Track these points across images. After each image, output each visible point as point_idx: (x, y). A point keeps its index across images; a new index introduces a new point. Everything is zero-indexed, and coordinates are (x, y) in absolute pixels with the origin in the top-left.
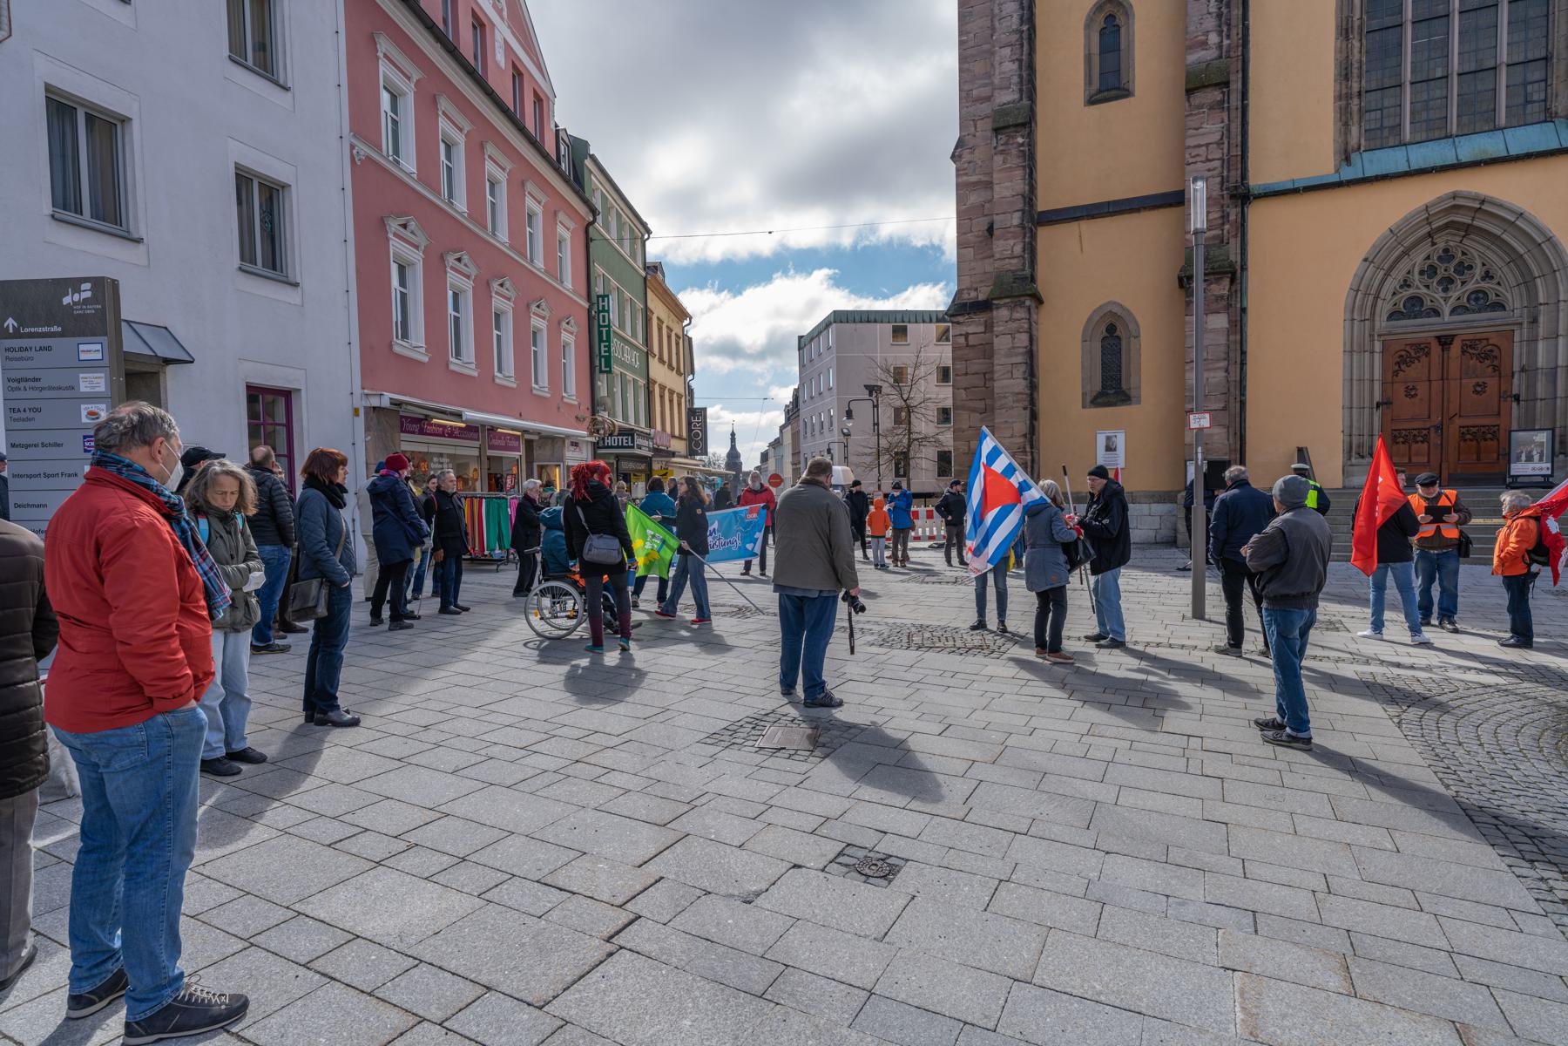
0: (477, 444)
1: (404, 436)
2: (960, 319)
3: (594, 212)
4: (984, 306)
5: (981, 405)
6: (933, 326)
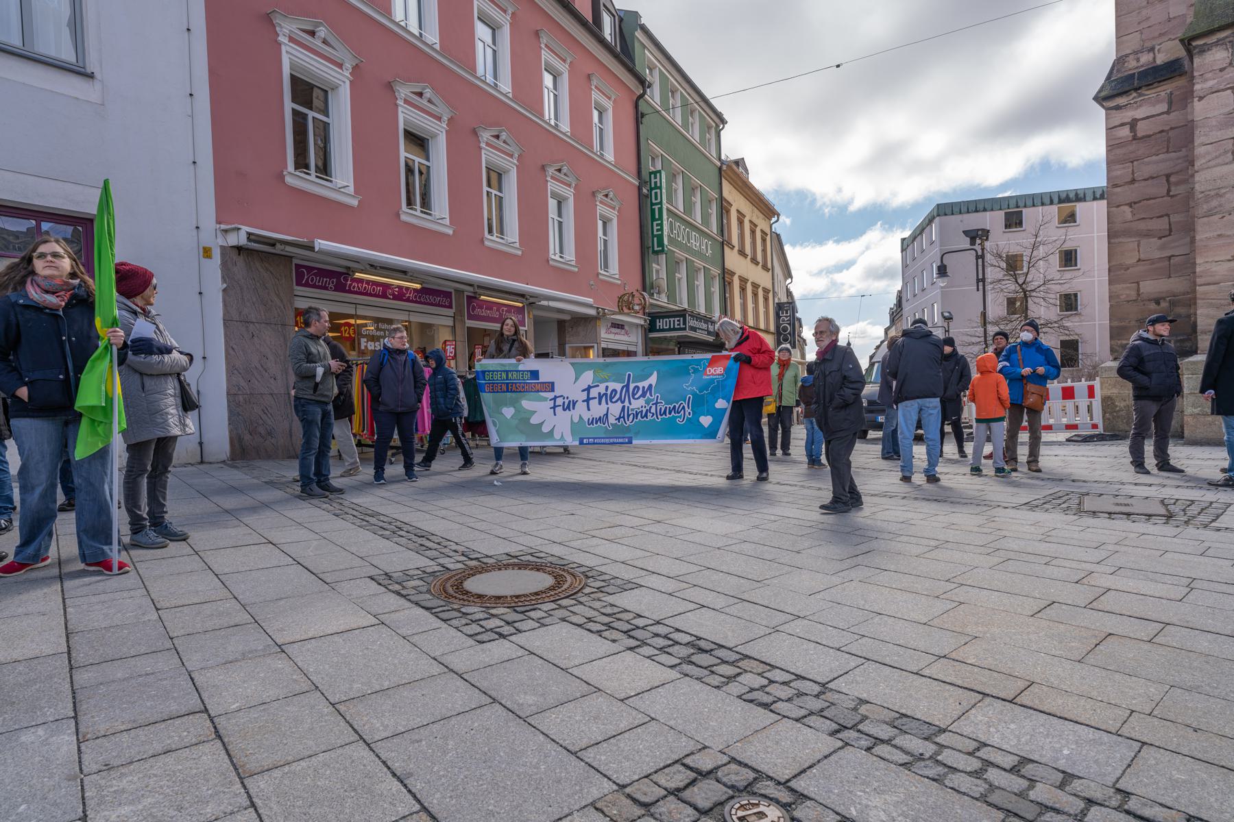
0: (451, 312)
1: (299, 290)
2: (1121, 101)
3: (642, 81)
4: (1172, 70)
5: (1163, 224)
6: (1055, 208)
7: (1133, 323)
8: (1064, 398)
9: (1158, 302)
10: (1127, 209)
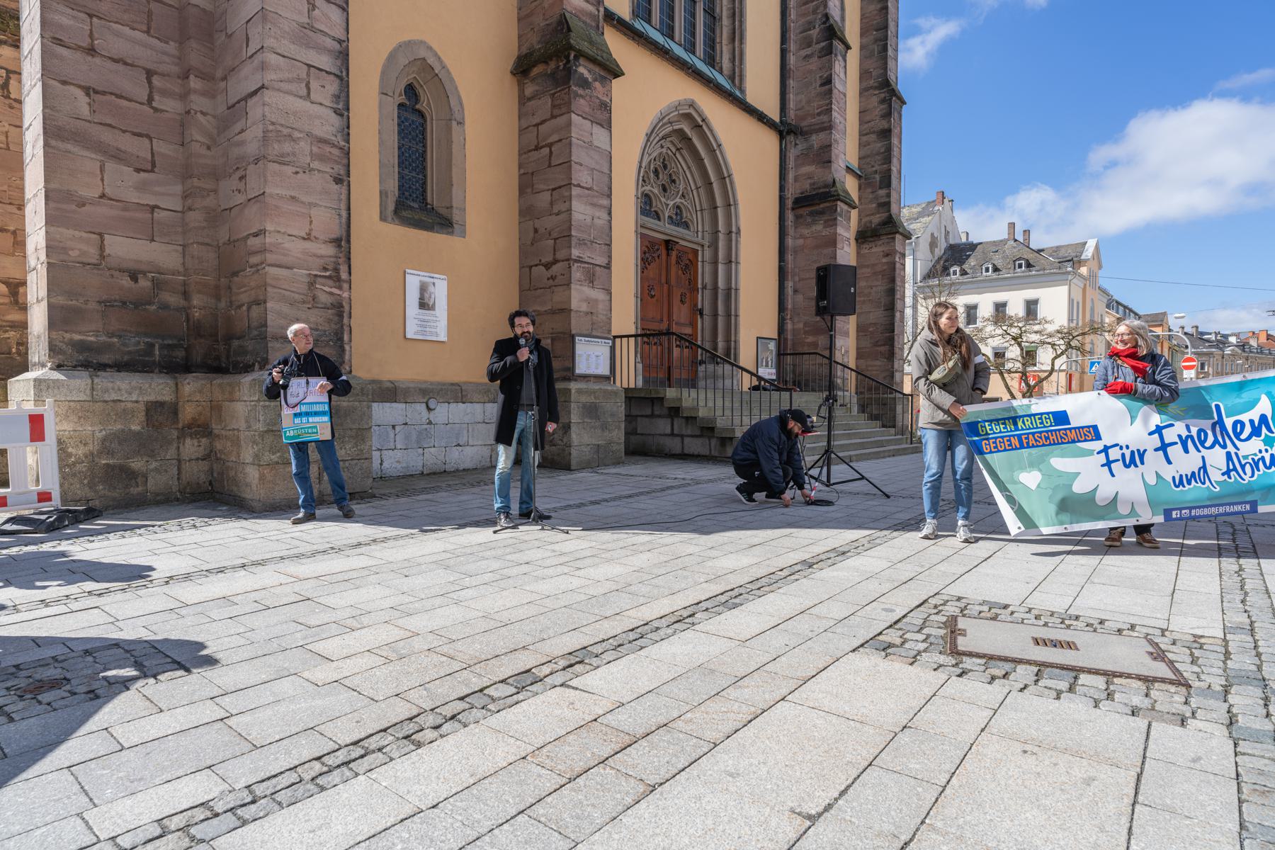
7: (92, 305)
8: (32, 440)
9: (134, 277)
10: (79, 93)
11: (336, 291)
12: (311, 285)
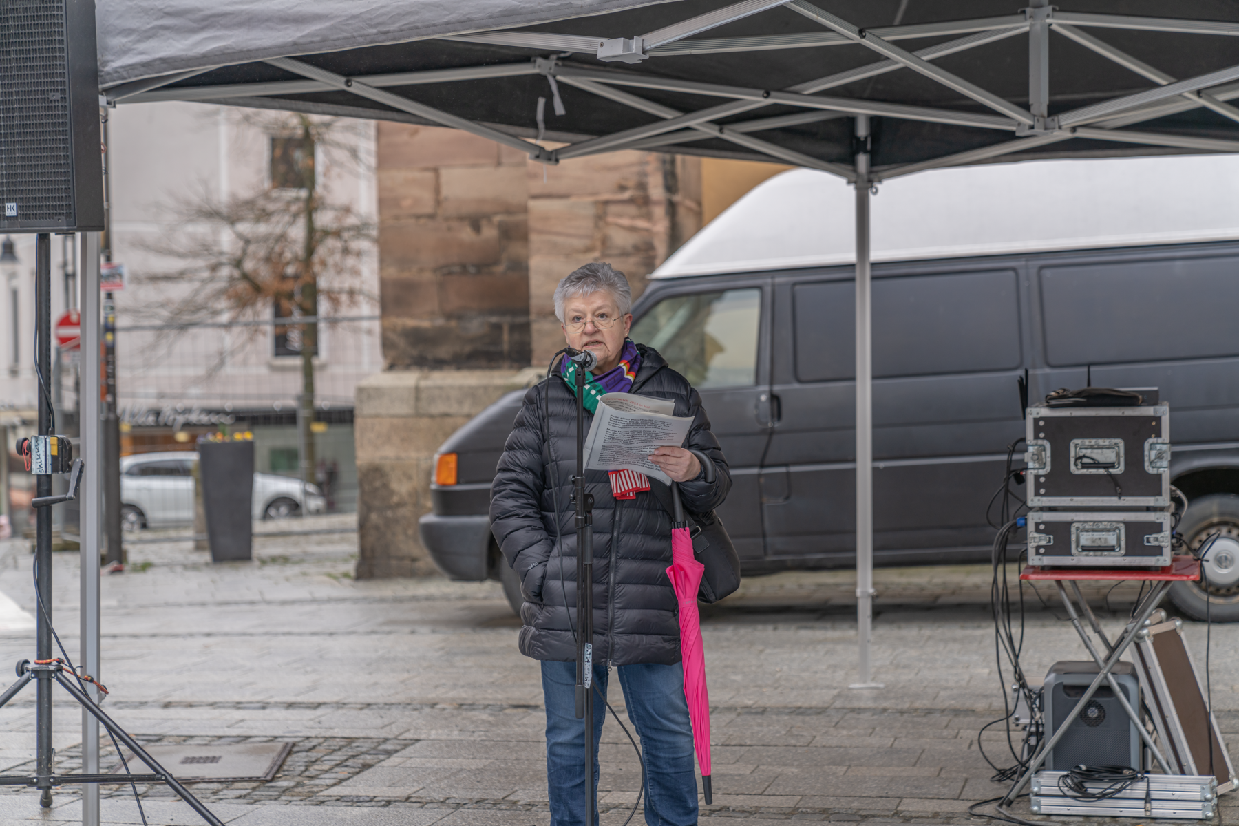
7: (427, 276)
9: (476, 227)
11: (641, 224)
12: (600, 218)
